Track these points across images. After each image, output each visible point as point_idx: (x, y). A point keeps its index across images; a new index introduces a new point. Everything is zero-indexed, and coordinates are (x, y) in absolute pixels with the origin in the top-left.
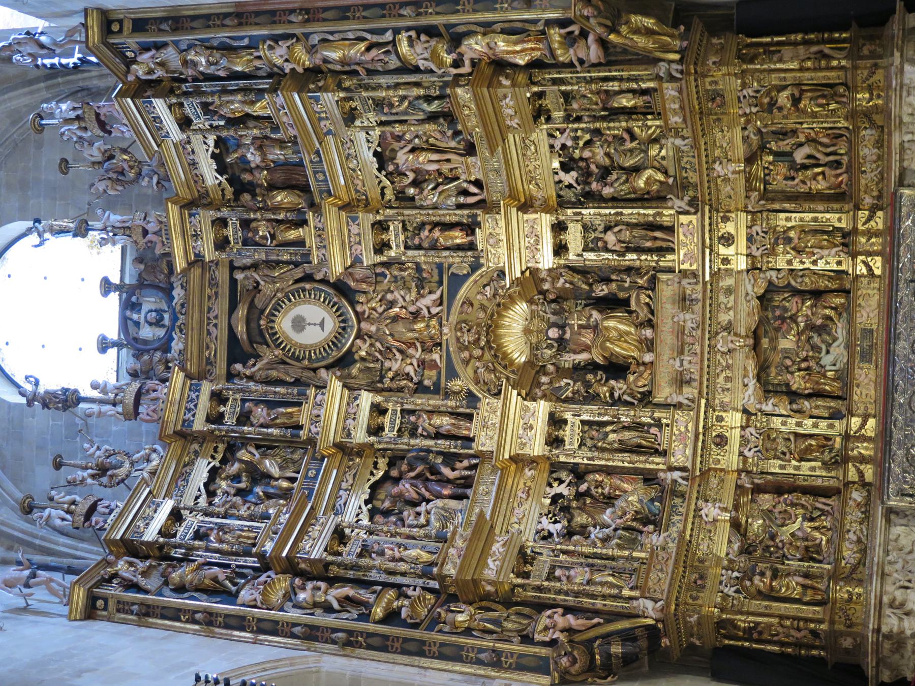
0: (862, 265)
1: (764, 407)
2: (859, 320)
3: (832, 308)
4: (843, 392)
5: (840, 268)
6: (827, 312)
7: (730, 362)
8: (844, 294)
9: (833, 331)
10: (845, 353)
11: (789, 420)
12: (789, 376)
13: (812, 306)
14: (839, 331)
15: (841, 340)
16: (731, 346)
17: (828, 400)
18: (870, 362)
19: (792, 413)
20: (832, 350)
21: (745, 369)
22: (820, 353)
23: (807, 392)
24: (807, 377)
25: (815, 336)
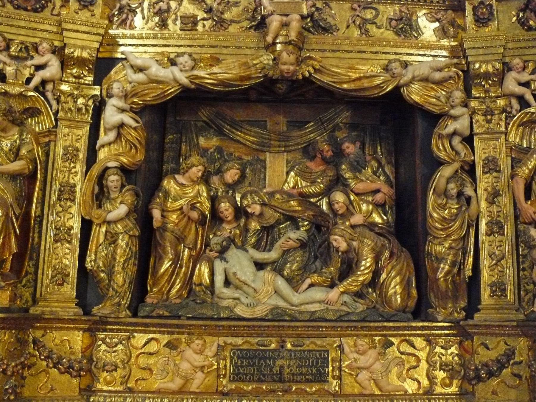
0: (502, 348)
1: (113, 103)
2: (348, 342)
3: (376, 273)
4: (154, 306)
5: (485, 293)
6: (367, 263)
7: (233, 29)
8: (412, 303)
9: (316, 278)
10: (260, 311)
11: (80, 167)
12: (196, 171)
13: (371, 226)
14: (318, 294)
15: (296, 298)
16: (275, 22)
17: (132, 269)
18: (236, 377)
19: (96, 170)
20: (267, 275)
21: (215, 61)
22: (257, 246)
23: (156, 213)
24: (195, 215)
25: (301, 234)
